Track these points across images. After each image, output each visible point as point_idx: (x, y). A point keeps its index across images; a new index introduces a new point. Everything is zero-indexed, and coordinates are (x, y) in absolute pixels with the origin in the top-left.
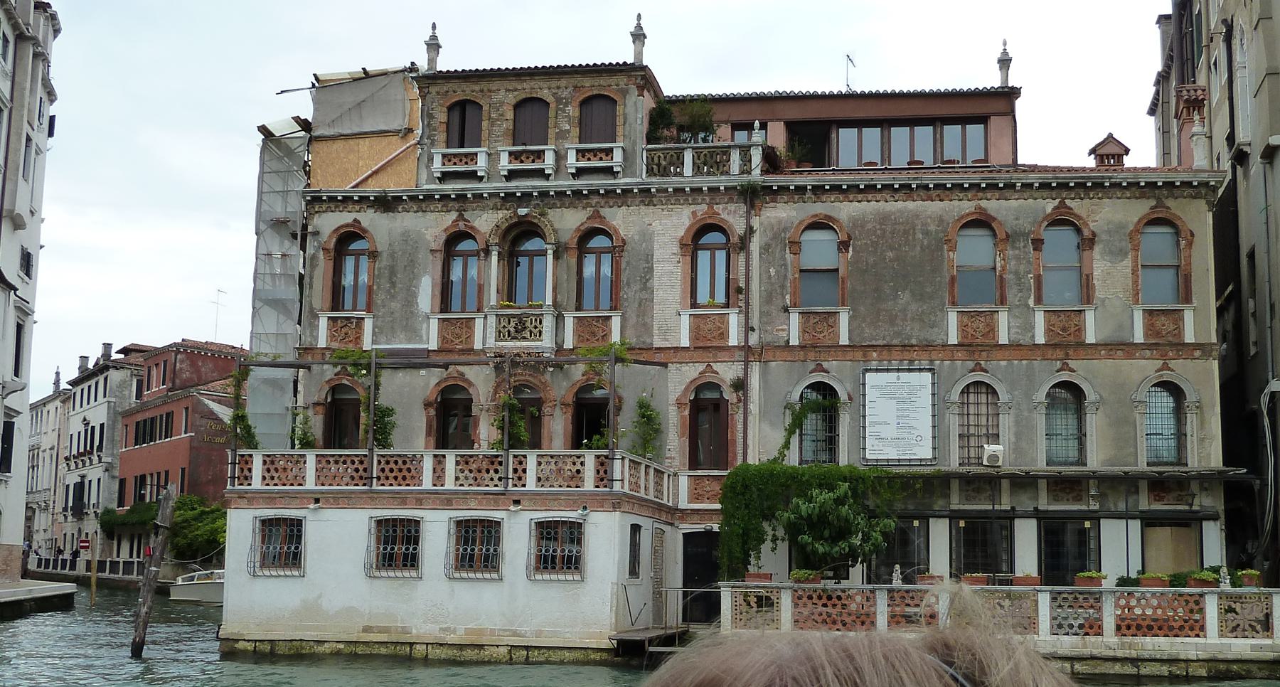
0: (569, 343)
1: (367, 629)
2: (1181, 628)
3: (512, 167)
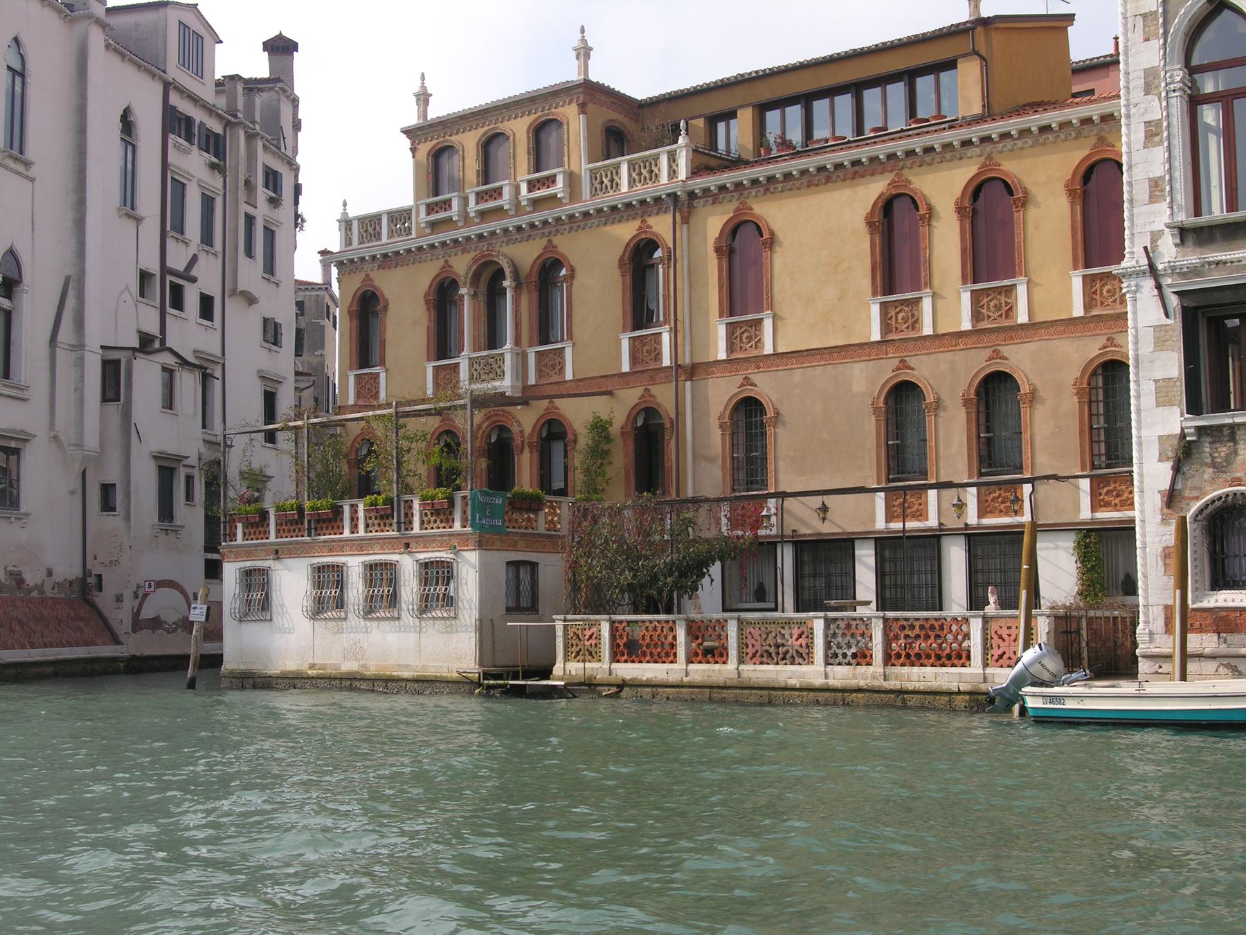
0: (532, 380)
1: (312, 666)
2: (949, 657)
3: (480, 207)
